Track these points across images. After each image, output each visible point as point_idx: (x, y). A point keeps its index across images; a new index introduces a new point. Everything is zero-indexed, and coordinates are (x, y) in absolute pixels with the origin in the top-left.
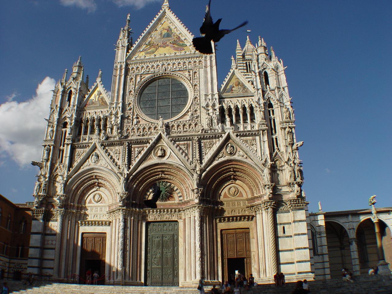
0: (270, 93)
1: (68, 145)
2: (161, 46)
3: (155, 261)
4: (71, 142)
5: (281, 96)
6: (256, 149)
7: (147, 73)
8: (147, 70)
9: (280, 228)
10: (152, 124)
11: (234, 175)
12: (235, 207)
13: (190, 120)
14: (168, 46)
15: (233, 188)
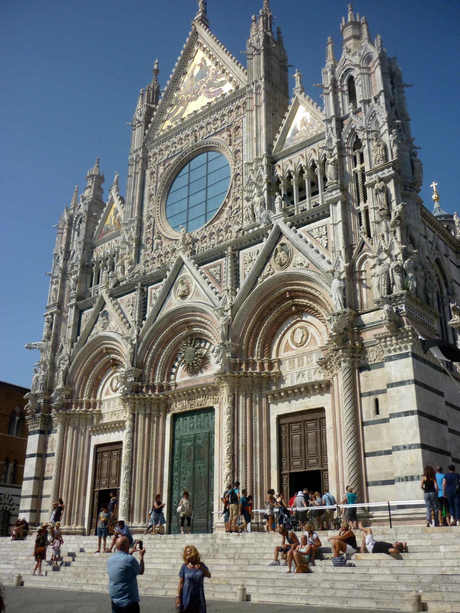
0: (353, 118)
1: (71, 307)
2: (191, 100)
3: (184, 484)
4: (74, 302)
5: (371, 118)
6: (327, 244)
7: (173, 155)
8: (173, 149)
9: (367, 404)
10: (176, 243)
11: (297, 305)
12: (302, 367)
13: (227, 219)
14: (200, 94)
15: (298, 330)
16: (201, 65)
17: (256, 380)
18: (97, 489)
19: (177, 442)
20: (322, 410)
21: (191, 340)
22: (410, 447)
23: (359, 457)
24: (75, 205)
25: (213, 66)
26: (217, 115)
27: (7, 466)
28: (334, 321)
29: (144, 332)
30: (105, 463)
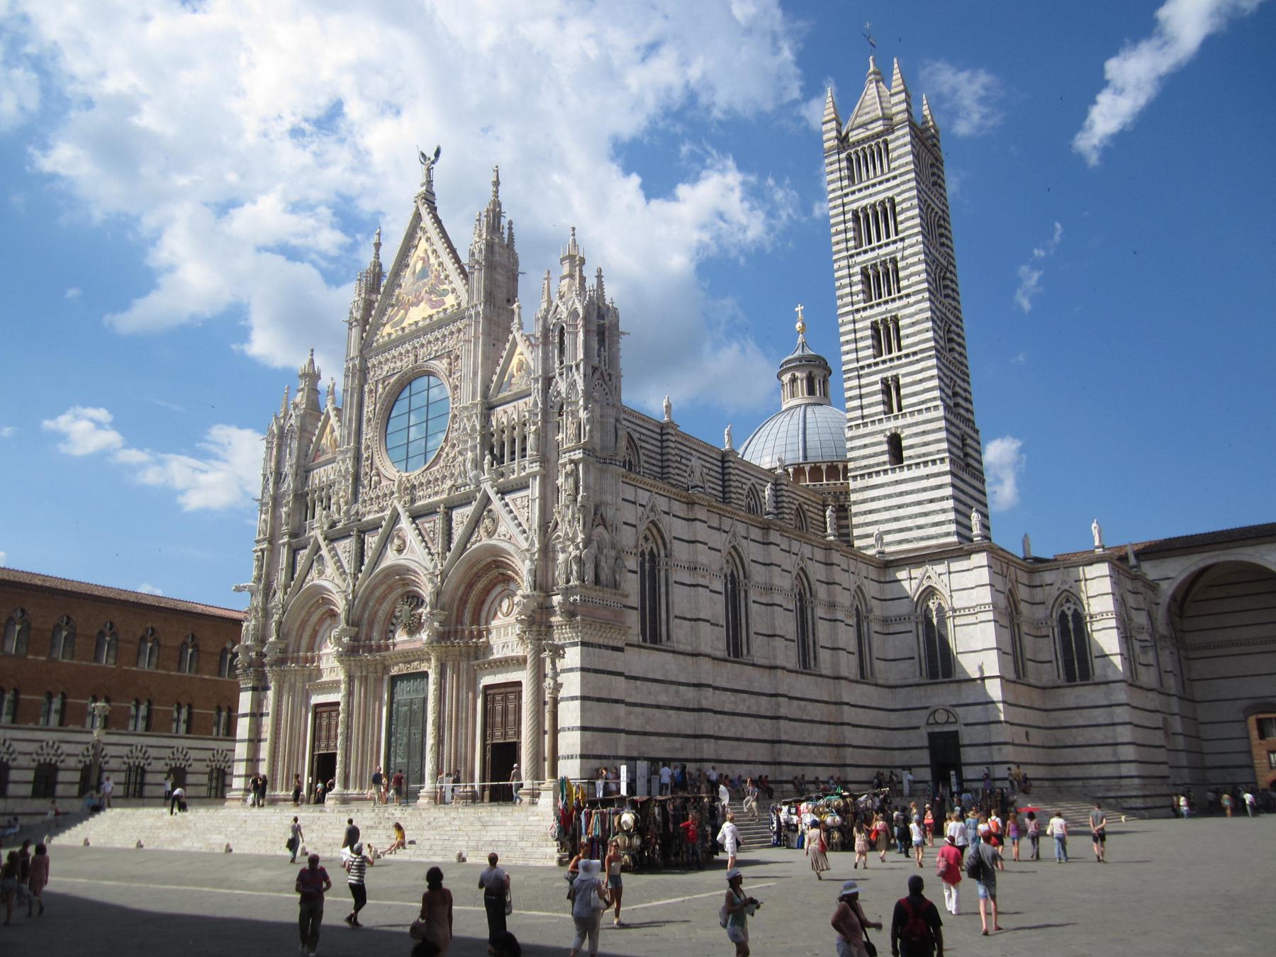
1: (284, 544)
8: (392, 365)
11: (503, 574)
14: (421, 301)
16: (423, 259)
17: (463, 650)
18: (316, 753)
19: (395, 706)
20: (519, 684)
21: (408, 598)
22: (573, 729)
23: (538, 733)
24: (286, 414)
25: (436, 266)
26: (437, 334)
27: (219, 716)
28: (508, 614)
29: (360, 586)
30: (324, 723)
